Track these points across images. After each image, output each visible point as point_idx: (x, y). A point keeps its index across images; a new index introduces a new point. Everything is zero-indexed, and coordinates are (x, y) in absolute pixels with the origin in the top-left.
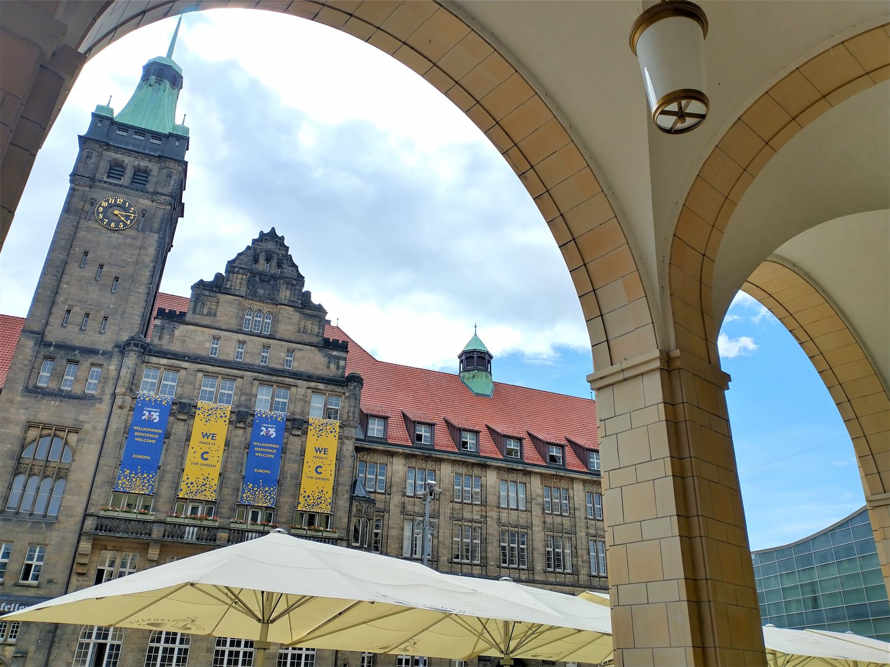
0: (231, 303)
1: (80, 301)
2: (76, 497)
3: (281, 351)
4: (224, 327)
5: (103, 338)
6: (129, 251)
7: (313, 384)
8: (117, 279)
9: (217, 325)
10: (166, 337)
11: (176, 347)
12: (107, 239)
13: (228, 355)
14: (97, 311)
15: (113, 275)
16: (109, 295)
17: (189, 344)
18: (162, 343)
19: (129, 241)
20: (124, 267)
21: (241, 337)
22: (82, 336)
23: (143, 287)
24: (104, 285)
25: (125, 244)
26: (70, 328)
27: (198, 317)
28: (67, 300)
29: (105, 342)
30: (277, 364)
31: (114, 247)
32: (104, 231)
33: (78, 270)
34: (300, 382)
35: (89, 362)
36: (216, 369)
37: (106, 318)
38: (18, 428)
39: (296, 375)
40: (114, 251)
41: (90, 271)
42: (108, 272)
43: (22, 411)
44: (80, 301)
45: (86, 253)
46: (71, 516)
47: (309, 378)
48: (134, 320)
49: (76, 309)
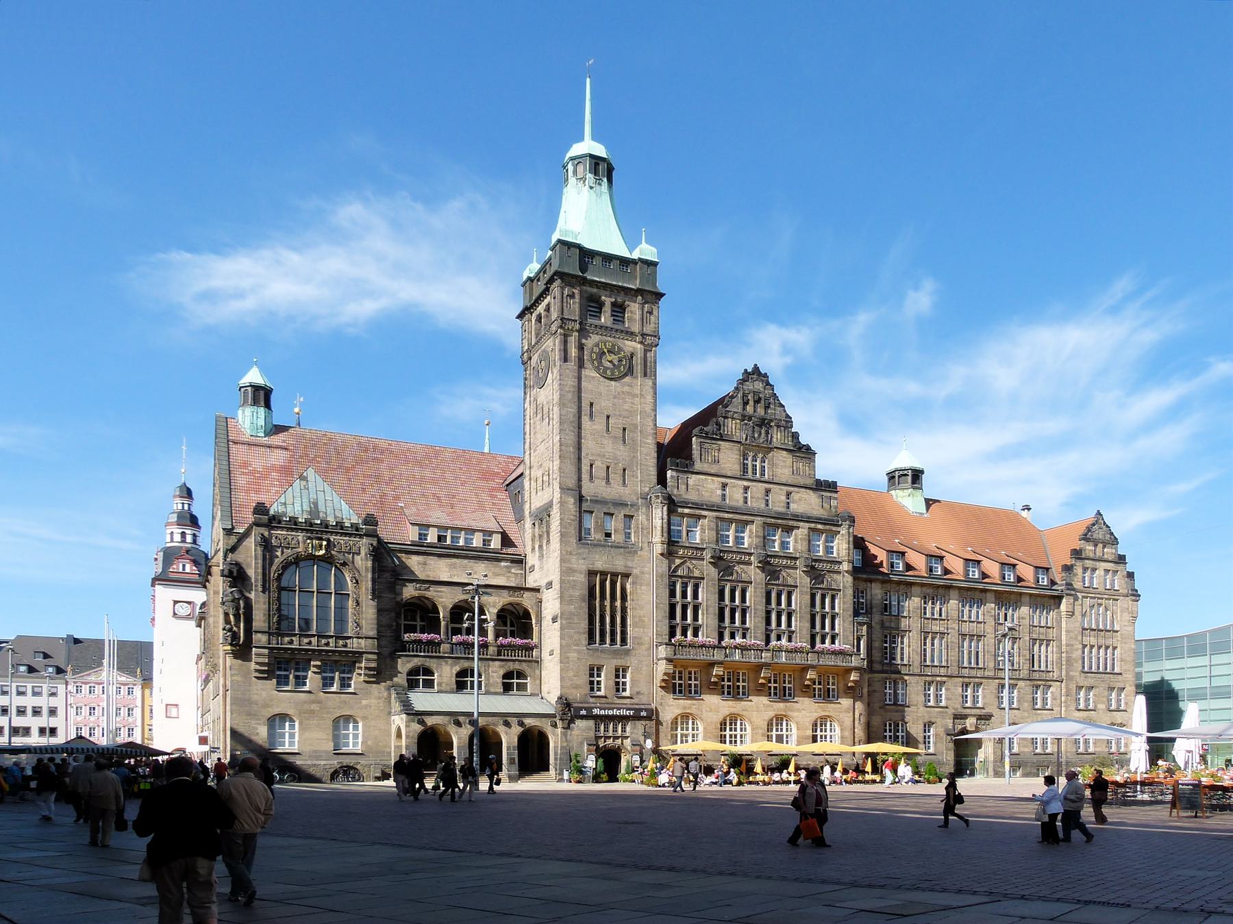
0: (732, 449)
1: (599, 455)
2: (642, 630)
3: (782, 495)
4: (729, 474)
5: (627, 491)
6: (630, 400)
7: (813, 525)
8: (624, 429)
9: (724, 472)
10: (683, 487)
11: (692, 496)
12: (607, 389)
13: (738, 501)
14: (616, 464)
15: (621, 426)
16: (622, 447)
17: (703, 493)
18: (681, 493)
19: (626, 389)
20: (628, 418)
21: (746, 483)
22: (609, 490)
23: (651, 438)
24: (615, 437)
25: (623, 392)
26: (596, 481)
27: (706, 465)
28: (588, 454)
29: (629, 494)
30: (779, 507)
31: (615, 397)
32: (602, 379)
33: (589, 423)
34: (801, 524)
35: (623, 514)
36: (730, 516)
37: (624, 470)
38: (583, 576)
39: (798, 518)
40: (616, 400)
41: (599, 424)
42: (615, 423)
43: (581, 561)
44: (599, 455)
45: (591, 404)
46: (642, 644)
47: (808, 519)
48: (651, 471)
49: (598, 464)
